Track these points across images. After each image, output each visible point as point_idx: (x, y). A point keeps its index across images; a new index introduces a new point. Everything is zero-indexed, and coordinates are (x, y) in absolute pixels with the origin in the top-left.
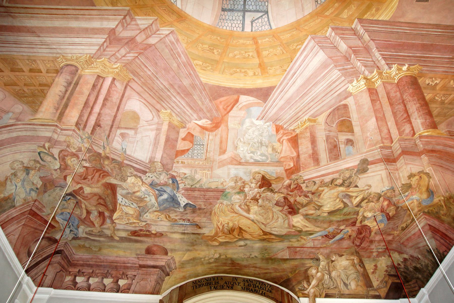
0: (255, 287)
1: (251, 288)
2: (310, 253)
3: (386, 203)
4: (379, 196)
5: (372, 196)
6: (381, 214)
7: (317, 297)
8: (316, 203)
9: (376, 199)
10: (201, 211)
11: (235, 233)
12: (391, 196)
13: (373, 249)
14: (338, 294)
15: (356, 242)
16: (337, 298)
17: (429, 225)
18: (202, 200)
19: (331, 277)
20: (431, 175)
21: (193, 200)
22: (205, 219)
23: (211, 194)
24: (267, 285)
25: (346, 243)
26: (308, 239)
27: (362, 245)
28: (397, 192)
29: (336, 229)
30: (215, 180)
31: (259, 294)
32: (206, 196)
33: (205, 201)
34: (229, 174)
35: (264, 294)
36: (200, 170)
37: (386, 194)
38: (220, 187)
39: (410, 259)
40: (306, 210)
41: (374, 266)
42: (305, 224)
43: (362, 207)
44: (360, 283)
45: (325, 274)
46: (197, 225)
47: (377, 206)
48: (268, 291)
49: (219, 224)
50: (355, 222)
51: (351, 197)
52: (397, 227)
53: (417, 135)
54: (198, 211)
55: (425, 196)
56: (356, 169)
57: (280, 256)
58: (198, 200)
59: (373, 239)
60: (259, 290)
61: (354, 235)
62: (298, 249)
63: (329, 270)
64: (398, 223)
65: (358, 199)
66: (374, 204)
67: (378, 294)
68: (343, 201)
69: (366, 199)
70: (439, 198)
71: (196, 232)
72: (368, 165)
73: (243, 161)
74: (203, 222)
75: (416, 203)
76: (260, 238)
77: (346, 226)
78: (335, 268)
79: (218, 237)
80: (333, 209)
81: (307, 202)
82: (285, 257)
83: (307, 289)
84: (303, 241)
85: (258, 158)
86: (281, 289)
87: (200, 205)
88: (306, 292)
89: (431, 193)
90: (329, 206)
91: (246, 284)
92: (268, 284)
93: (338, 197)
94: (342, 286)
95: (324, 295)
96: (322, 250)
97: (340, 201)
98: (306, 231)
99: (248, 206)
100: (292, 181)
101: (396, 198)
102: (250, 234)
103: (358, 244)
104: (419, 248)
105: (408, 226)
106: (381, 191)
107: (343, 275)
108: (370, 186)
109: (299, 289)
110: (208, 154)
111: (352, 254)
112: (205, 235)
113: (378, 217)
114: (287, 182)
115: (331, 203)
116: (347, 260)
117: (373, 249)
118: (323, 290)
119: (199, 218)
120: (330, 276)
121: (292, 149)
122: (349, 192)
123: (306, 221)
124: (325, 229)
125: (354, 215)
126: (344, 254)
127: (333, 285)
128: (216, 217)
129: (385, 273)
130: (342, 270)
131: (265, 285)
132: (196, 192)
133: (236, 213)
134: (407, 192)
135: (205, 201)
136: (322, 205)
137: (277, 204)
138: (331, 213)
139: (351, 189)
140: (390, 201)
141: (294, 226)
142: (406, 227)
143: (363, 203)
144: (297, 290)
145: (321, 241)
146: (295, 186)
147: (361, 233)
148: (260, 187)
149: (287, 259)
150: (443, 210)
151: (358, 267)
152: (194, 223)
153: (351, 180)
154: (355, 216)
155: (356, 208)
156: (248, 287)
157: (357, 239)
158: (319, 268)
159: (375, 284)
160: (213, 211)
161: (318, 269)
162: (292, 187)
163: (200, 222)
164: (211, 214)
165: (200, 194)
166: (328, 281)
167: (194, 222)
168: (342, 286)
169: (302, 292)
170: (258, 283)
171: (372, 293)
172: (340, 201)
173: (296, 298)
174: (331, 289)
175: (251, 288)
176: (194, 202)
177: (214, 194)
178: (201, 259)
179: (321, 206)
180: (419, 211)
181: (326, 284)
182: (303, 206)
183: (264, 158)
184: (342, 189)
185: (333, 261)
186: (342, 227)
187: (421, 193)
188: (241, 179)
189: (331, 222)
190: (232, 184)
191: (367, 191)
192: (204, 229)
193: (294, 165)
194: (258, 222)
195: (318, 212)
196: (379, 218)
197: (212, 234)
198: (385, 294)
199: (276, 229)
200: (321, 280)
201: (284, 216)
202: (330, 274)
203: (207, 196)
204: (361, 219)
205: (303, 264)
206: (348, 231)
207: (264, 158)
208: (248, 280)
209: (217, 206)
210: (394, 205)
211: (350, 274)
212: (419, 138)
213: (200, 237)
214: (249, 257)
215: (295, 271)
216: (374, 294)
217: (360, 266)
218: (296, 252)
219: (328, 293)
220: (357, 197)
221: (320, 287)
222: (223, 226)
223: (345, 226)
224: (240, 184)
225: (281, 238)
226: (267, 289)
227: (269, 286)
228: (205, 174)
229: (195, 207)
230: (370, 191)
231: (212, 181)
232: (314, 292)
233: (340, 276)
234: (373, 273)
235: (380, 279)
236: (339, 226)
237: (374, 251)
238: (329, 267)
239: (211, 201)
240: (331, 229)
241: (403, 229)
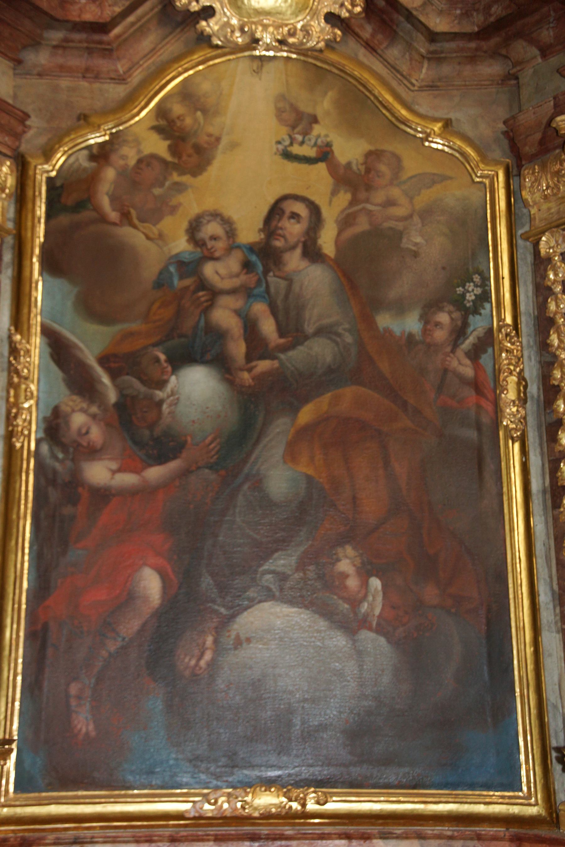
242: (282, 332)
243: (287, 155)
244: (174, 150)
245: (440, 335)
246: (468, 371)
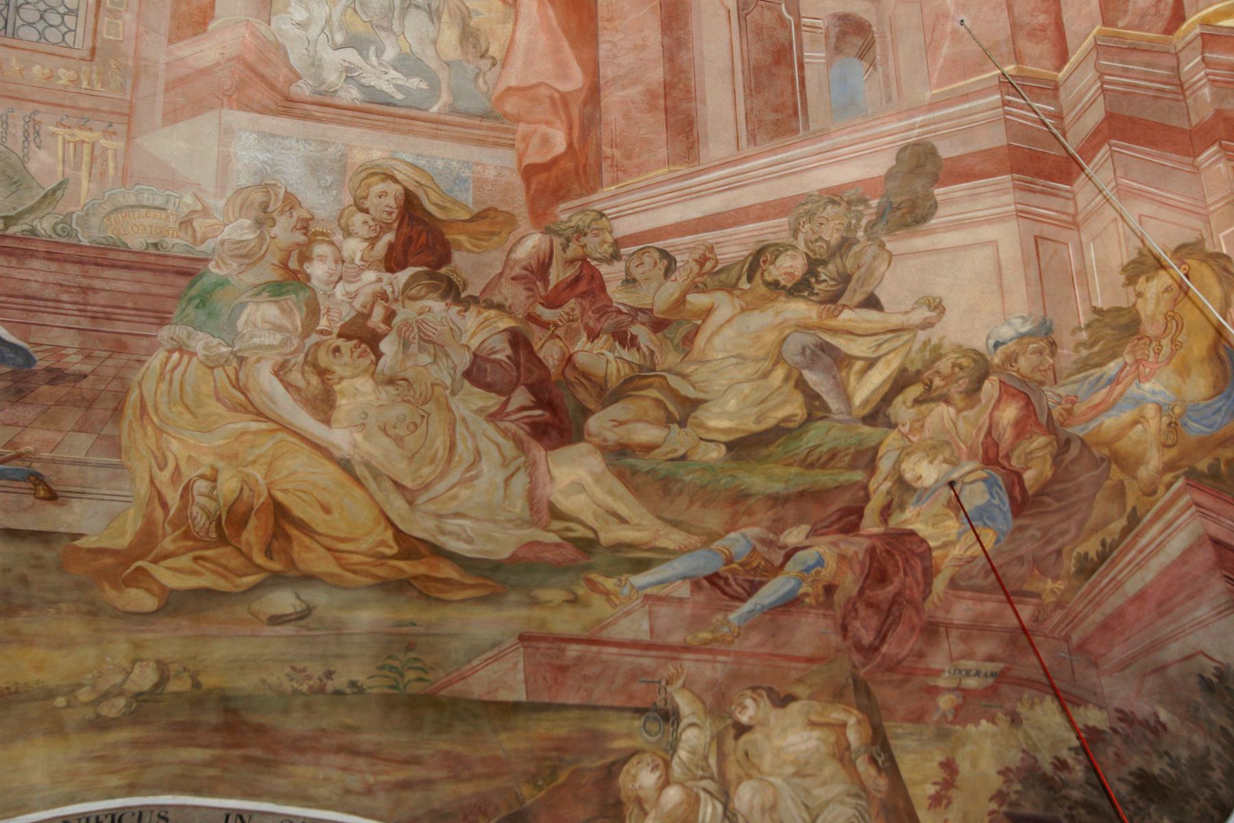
2: (635, 675)
3: (1010, 413)
5: (944, 366)
6: (984, 474)
8: (673, 381)
9: (964, 384)
10: (62, 390)
11: (252, 535)
12: (1038, 376)
13: (938, 673)
15: (857, 624)
17: (1216, 542)
18: (72, 321)
21: (17, 316)
22: (85, 440)
23: (120, 282)
26: (626, 591)
27: (884, 649)
28: (1067, 354)
29: (763, 541)
30: (146, 199)
32: (92, 298)
33: (85, 323)
34: (224, 165)
36: (60, 124)
37: (1011, 359)
38: (177, 243)
39: (1115, 730)
40: (621, 423)
41: (942, 765)
42: (610, 501)
43: (892, 426)
45: (702, 795)
46: (37, 479)
49: (164, 477)
50: (858, 512)
51: (841, 360)
52: (1059, 552)
53: (1191, 27)
54: (44, 388)
56: (874, 203)
57: (478, 686)
58: (48, 319)
59: (940, 615)
61: (850, 583)
63: (722, 773)
64: (1062, 534)
65: (878, 378)
66: (952, 410)
68: (801, 385)
71: (27, 522)
72: (936, 180)
73: (303, 89)
74: (74, 463)
75: (1153, 425)
76: (381, 572)
77: (814, 532)
79: (155, 561)
81: (626, 371)
82: (504, 696)
85: (388, 82)
87: (57, 350)
90: (732, 404)
93: (779, 360)
96: (689, 663)
97: (787, 379)
98: (618, 547)
99: (322, 373)
100: (557, 242)
101: (1062, 391)
102: (329, 549)
103: (867, 638)
104: (1161, 669)
105: (1112, 549)
106: (992, 342)
107: (790, 804)
108: (938, 307)
110: (105, 20)
111: (837, 695)
112: (80, 543)
113: (967, 489)
114: (531, 243)
115: (746, 388)
116: (813, 725)
117: (938, 673)
119: (49, 435)
120: (725, 806)
121: (565, 44)
122: (834, 331)
123: (620, 488)
124: (712, 537)
125: (852, 467)
126: (798, 690)
128: (150, 429)
129: (994, 806)
130: (786, 779)
132: (36, 264)
133: (260, 415)
134: (1113, 357)
135: (85, 323)
136: (701, 396)
137: (477, 373)
139: (846, 315)
140: (1029, 403)
141: (556, 514)
142: (1102, 557)
145: (687, 610)
146: (570, 272)
148: (392, 262)
149: (516, 707)
151: (862, 765)
152: (16, 464)
153: (849, 263)
154: (858, 476)
155: (866, 430)
157: (862, 612)
158: (676, 760)
160: (134, 397)
161: (667, 765)
162: (557, 274)
163: (53, 461)
164: (118, 412)
165: (60, 278)
167: (19, 456)
172: (791, 383)
176: (21, 327)
177: (137, 288)
178: (51, 694)
179: (695, 404)
180: (1169, 467)
182: (610, 395)
183: (415, 83)
184: (800, 309)
185: (741, 730)
186: (793, 537)
187: (1184, 371)
188: (291, 202)
190: (241, 230)
191: (922, 335)
192: (77, 506)
193: (570, 145)
194: (377, 475)
195: (679, 439)
196: (975, 496)
197: (123, 542)
199: (466, 523)
201: (509, 447)
202: (725, 796)
203: (101, 299)
204: (888, 493)
205: (597, 738)
206: (820, 562)
207: (415, 83)
209: (156, 361)
210: (1051, 428)
211: (827, 803)
212: (1199, 40)
213: (50, 555)
214: (321, 690)
215: (554, 772)
217: (873, 760)
218: (563, 669)
220: (871, 363)
222: (187, 489)
223: (806, 528)
224: (283, 232)
228: (86, 149)
229: (29, 359)
230: (934, 335)
231: (132, 200)
233: (773, 808)
234: (937, 801)
236: (779, 526)
237: (941, 682)
238: (722, 757)
239: (122, 327)
240: (739, 541)
241: (1087, 568)
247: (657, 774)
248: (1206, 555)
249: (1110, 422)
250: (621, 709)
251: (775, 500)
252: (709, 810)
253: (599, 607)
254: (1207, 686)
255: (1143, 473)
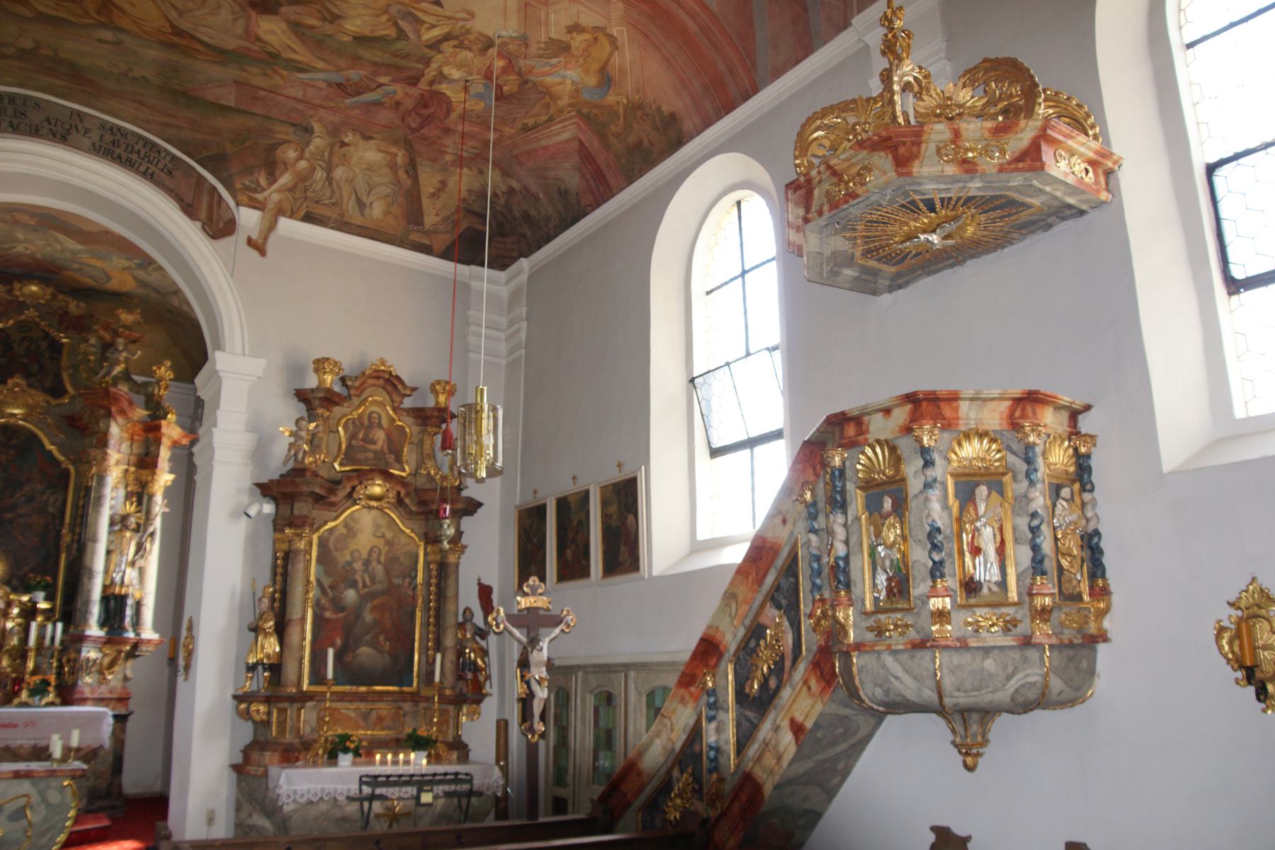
0: (131, 152)
1: (118, 151)
3: (499, 64)
4: (488, 44)
5: (471, 37)
6: (484, 82)
7: (284, 215)
9: (479, 46)
12: (518, 54)
13: (448, 147)
14: (336, 221)
15: (409, 119)
16: (332, 228)
17: (581, 142)
19: (329, 179)
20: (619, 44)
24: (163, 154)
25: (385, 116)
26: (293, 78)
27: (422, 131)
28: (533, 50)
29: (367, 77)
31: (137, 172)
35: (152, 175)
37: (505, 44)
39: (521, 192)
40: (298, 14)
42: (289, 42)
43: (440, 52)
44: (395, 209)
45: (318, 167)
47: (479, 62)
48: (162, 170)
52: (515, 119)
55: (592, 81)
57: (212, 94)
59: (452, 126)
60: (139, 160)
61: (409, 104)
62: (262, 93)
63: (330, 160)
64: (518, 113)
65: (435, 33)
66: (472, 55)
67: (427, 242)
68: (396, 24)
69: (456, 38)
70: (618, 98)
75: (569, 87)
77: (394, 80)
78: (345, 160)
80: (367, 32)
82: (224, 102)
83: (264, 190)
84: (277, 78)
86: (198, 173)
88: (260, 197)
89: (606, 79)
90: (358, 22)
91: (108, 138)
92: (168, 153)
93: (386, 12)
94: (350, 206)
95: (302, 213)
96: (322, 112)
97: (389, 20)
101: (528, 62)
103: (414, 125)
104: (546, 178)
105: (539, 126)
106: (496, 36)
107: (360, 181)
109: (244, 184)
111: (395, 142)
113: (474, 85)
115: (367, 18)
116: (381, 151)
117: (448, 147)
118: (303, 203)
120: (328, 174)
122: (417, 9)
123: (294, 38)
124: (340, 69)
125: (418, 61)
126: (375, 136)
127: (331, 198)
131: (159, 152)
134: (555, 57)
136: (343, 15)
138: (360, 40)
140: (510, 62)
141: (258, 39)
142: (534, 128)
143: (445, 44)
144: (238, 186)
147: (426, 106)
149: (229, 108)
150: (616, 125)
151: (401, 173)
154: (420, 66)
155: (427, 51)
156: (110, 146)
157: (413, 115)
158: (307, 150)
159: (430, 220)
161: (303, 151)
166: (320, 184)
168: (350, 206)
169: (251, 194)
170: (141, 143)
171: (415, 237)
172: (391, 23)
173: (232, 203)
174: (323, 204)
175: (118, 151)
179: (339, 17)
180: (571, 105)
181: (314, 192)
185: (343, 144)
186: (383, 80)
187: (587, 72)
189: (356, 60)
191: (461, 23)
196: (477, 88)
198: (444, 247)
199: (210, 31)
200: (303, 179)
201: (237, 8)
202: (329, 170)
204: (434, 76)
206: (395, 92)
208: (113, 129)
210: (520, 74)
211: (380, 184)
216: (417, 239)
217: (407, 172)
218: (257, 99)
219: (315, 211)
220: (433, 26)
221: (298, 194)
223: (390, 78)
225: (222, 55)
226: (161, 165)
227: (168, 158)
230: (468, 25)
232: (280, 202)
233: (352, 180)
234: (433, 195)
235: (444, 213)
236: (376, 74)
237: (448, 150)
238: (331, 154)
240: (355, 74)
241: (526, 129)
242: (371, 581)
243: (374, 535)
244: (348, 532)
245: (406, 584)
246: (411, 593)
247: (296, 153)
248: (575, 145)
249: (549, 80)
250: (284, 122)
251: (375, 64)
252: (320, 174)
253: (277, 80)
254: (560, 193)
255: (560, 103)
